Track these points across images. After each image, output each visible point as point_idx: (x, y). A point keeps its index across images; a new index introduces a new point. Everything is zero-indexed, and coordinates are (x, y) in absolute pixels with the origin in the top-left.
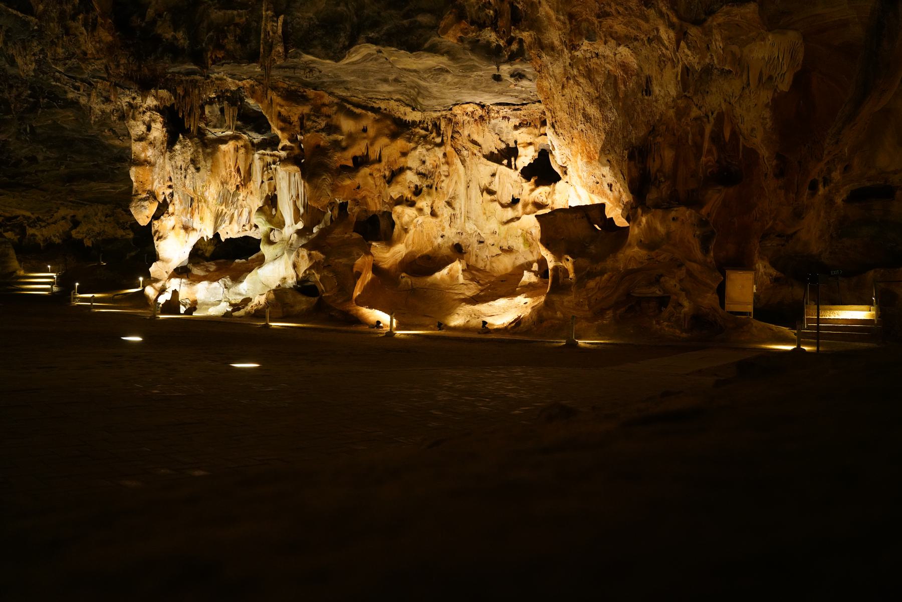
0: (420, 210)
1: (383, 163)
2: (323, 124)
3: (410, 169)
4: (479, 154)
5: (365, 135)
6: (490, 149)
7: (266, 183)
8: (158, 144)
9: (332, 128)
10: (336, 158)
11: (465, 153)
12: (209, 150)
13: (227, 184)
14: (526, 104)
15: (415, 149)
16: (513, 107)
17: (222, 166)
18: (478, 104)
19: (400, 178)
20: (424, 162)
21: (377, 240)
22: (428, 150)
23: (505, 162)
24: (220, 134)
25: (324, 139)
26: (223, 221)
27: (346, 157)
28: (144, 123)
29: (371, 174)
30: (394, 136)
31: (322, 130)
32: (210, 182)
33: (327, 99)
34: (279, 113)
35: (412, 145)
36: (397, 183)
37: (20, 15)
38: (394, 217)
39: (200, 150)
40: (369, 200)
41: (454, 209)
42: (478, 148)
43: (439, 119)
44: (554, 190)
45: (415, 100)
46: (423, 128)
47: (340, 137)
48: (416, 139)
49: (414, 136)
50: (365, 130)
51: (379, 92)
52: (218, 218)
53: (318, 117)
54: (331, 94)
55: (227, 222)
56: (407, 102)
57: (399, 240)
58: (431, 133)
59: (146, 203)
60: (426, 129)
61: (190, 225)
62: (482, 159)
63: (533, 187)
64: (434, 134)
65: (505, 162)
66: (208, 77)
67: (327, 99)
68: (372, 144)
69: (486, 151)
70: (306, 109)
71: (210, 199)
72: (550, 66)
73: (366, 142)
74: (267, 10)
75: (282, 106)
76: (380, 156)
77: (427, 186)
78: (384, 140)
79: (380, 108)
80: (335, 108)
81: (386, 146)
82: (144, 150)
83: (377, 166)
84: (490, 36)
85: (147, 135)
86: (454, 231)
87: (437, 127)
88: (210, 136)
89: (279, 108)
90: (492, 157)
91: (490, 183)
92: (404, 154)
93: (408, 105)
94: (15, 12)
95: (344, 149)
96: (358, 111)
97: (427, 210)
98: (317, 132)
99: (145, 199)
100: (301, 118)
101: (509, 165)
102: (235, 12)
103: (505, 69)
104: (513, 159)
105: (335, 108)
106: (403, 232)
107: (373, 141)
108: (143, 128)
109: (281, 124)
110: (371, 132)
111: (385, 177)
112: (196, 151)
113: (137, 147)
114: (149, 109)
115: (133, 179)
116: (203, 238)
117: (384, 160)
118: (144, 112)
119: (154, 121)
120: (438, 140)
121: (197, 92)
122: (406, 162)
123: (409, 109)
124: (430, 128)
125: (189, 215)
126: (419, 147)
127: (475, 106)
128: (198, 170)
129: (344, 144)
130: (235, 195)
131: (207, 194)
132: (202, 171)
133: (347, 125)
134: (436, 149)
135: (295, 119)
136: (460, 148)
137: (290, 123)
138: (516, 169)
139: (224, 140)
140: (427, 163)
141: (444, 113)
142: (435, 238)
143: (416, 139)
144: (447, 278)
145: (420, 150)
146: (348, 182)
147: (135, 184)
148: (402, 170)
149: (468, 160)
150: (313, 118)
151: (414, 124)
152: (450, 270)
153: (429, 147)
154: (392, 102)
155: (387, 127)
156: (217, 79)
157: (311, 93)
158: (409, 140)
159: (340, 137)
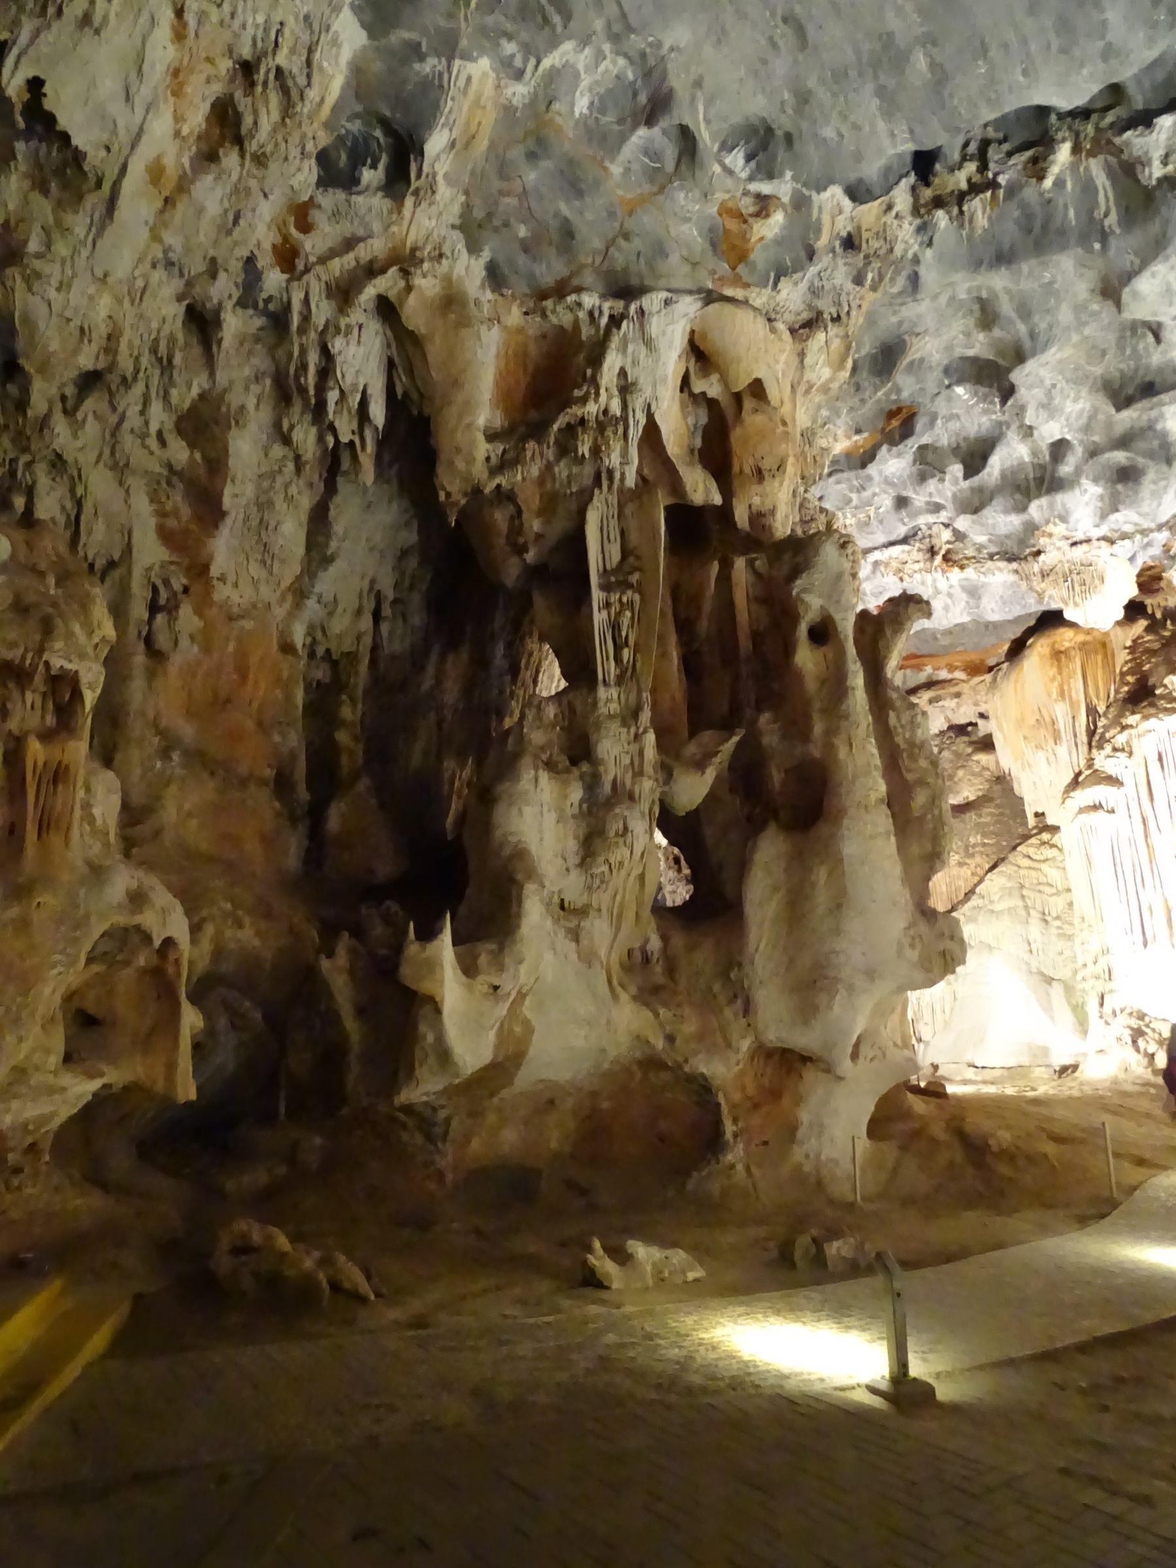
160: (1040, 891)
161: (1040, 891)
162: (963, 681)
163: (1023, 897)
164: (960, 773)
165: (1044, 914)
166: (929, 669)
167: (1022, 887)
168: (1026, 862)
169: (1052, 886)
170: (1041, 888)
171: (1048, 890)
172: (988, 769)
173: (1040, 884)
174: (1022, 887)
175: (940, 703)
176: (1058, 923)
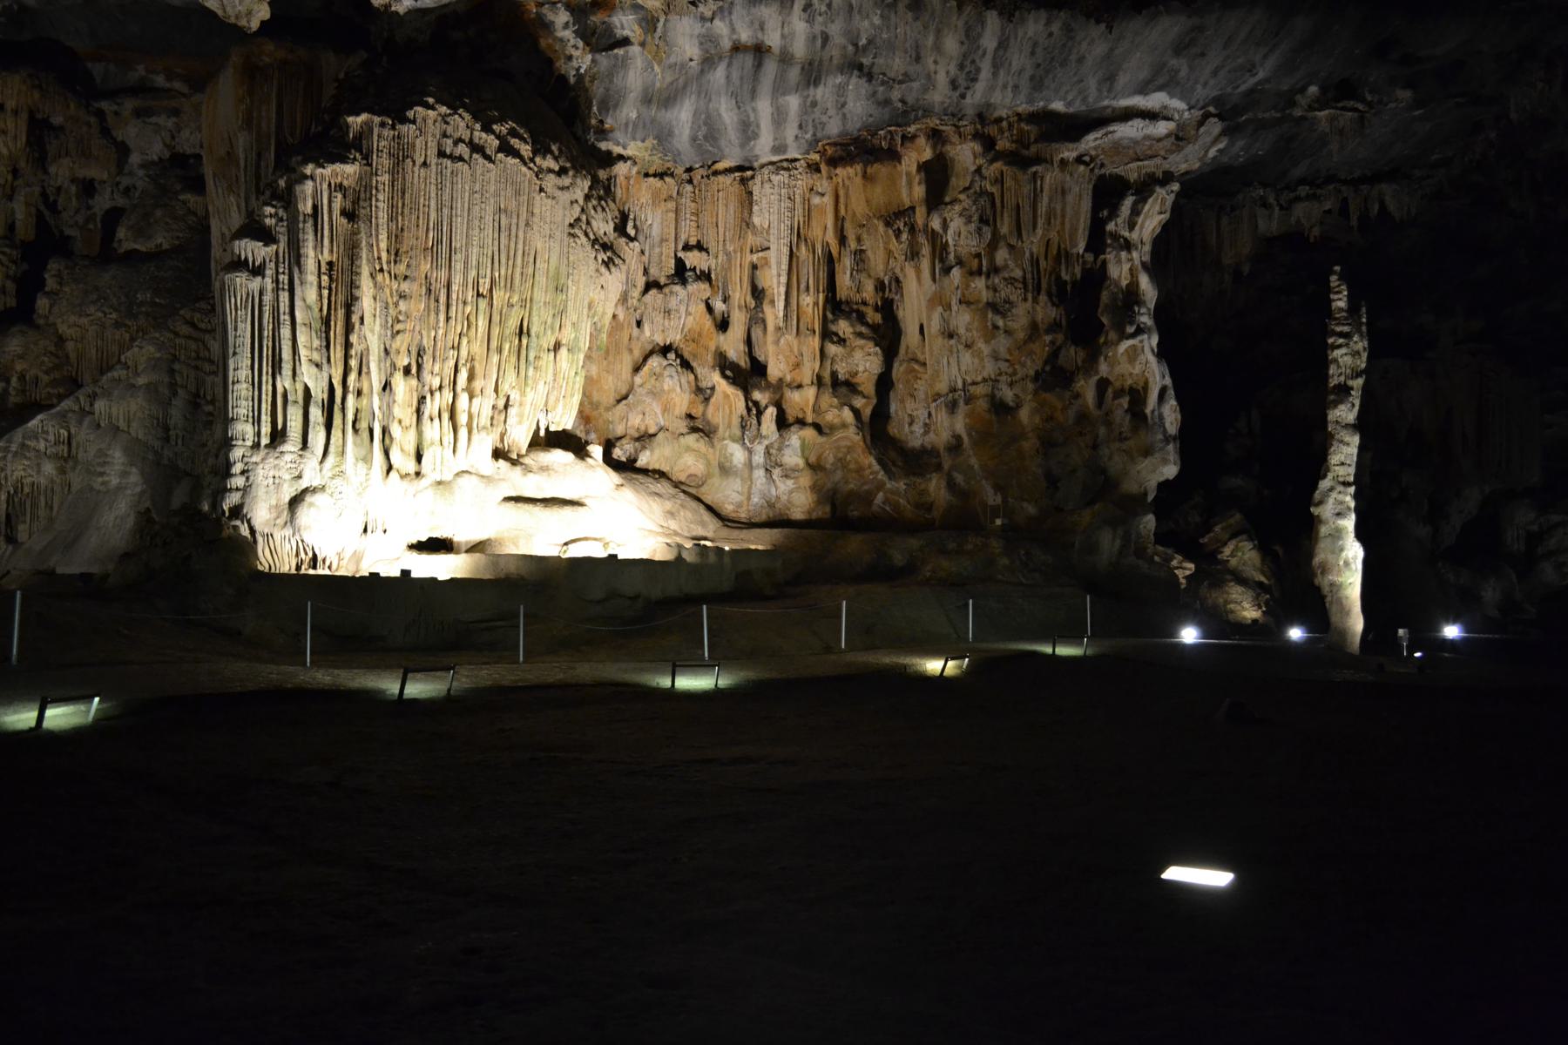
160: (196, 368)
161: (196, 368)
162: (184, 95)
163: (172, 372)
164: (159, 213)
165: (197, 395)
166: (141, 70)
167: (175, 359)
168: (185, 329)
169: (211, 362)
170: (199, 363)
171: (207, 367)
172: (195, 214)
173: (198, 358)
174: (175, 359)
175: (153, 119)
176: (210, 408)
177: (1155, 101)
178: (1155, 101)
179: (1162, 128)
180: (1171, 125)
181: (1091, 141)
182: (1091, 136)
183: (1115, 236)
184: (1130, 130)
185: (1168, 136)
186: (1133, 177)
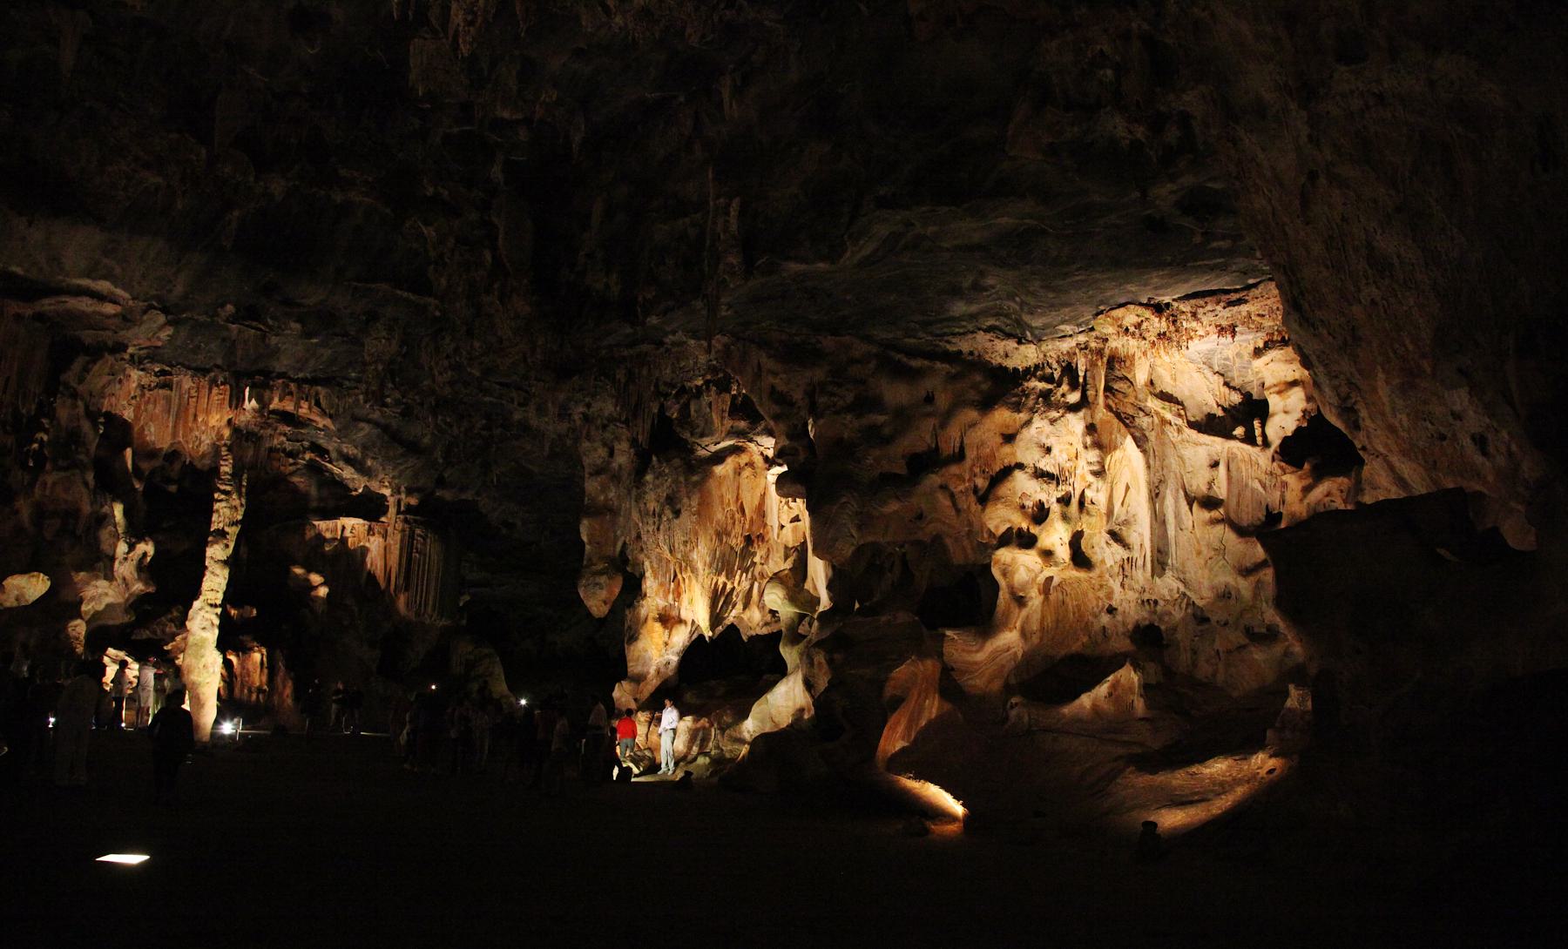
0: (1047, 554)
1: (968, 462)
2: (850, 398)
3: (1020, 466)
4: (1179, 421)
5: (929, 409)
6: (1206, 410)
7: (789, 526)
8: (625, 475)
9: (867, 403)
10: (870, 461)
11: (1144, 421)
12: (695, 478)
13: (728, 535)
14: (1255, 286)
15: (1028, 423)
16: (1224, 297)
17: (716, 501)
18: (1147, 306)
19: (1003, 490)
20: (1048, 450)
21: (953, 626)
22: (1053, 422)
23: (1239, 431)
24: (713, 448)
25: (849, 426)
26: (729, 602)
27: (893, 458)
28: (605, 445)
29: (944, 487)
30: (987, 405)
31: (849, 409)
32: (696, 534)
33: (860, 349)
34: (773, 387)
35: (1023, 416)
36: (998, 498)
37: (412, 297)
38: (996, 572)
39: (682, 479)
40: (948, 541)
41: (1126, 545)
42: (1175, 408)
43: (1071, 354)
44: (1358, 482)
45: (1019, 323)
46: (1043, 379)
47: (881, 419)
48: (1031, 403)
49: (1027, 396)
50: (929, 399)
51: (953, 319)
52: (719, 601)
53: (840, 385)
54: (868, 339)
55: (740, 606)
56: (1007, 329)
57: (1005, 625)
58: (1059, 385)
59: (603, 579)
60: (1049, 379)
61: (674, 613)
62: (1193, 434)
63: (1309, 481)
64: (1065, 387)
65: (1239, 431)
66: (662, 343)
67: (860, 349)
68: (943, 425)
69: (1195, 414)
70: (819, 374)
71: (700, 566)
72: (1261, 156)
73: (930, 423)
74: (718, 197)
75: (775, 374)
76: (962, 448)
77: (1059, 501)
78: (973, 414)
79: (960, 352)
80: (872, 365)
81: (973, 425)
82: (604, 489)
83: (954, 469)
84: (1116, 126)
85: (609, 463)
86: (1132, 596)
87: (1069, 370)
88: (702, 453)
89: (771, 379)
90: (1210, 425)
91: (1210, 485)
92: (1009, 438)
93: (1009, 336)
94: (405, 294)
95: (887, 441)
96: (916, 363)
97: (1063, 553)
98: (837, 413)
99: (600, 573)
100: (811, 394)
101: (1249, 439)
102: (687, 220)
103: (1165, 194)
104: (1256, 423)
105: (872, 365)
106: (1014, 606)
107: (946, 418)
108: (603, 452)
109: (776, 409)
110: (942, 401)
111: (976, 490)
112: (676, 481)
113: (591, 485)
114: (611, 420)
115: (585, 539)
116: (701, 636)
117: (971, 454)
118: (604, 427)
119: (618, 439)
120: (1074, 397)
121: (645, 372)
122: (1013, 454)
123: (1012, 344)
124: (1056, 376)
125: (671, 597)
126: (1036, 417)
127: (1140, 310)
128: (677, 513)
129: (887, 431)
130: (747, 553)
131: (695, 556)
132: (684, 515)
133: (896, 393)
134: (1070, 416)
135: (798, 395)
136: (1130, 411)
137: (792, 404)
138: (1266, 443)
139: (719, 458)
140: (1055, 451)
141: (1082, 338)
142: (1096, 616)
143: (1031, 403)
144: (1107, 707)
145: (1039, 423)
146: (893, 506)
147: (588, 547)
148: (1007, 472)
149: (1152, 436)
150: (830, 388)
151: (1029, 373)
152: (1114, 686)
153: (1054, 414)
154: (981, 336)
155: (975, 386)
156: (674, 344)
157: (828, 342)
158: (1017, 408)
159: (881, 419)
177: (104, 286)
178: (104, 286)
179: (109, 309)
180: (119, 309)
181: (47, 305)
182: (46, 301)
183: (67, 386)
184: (85, 305)
185: (115, 315)
186: (88, 341)
